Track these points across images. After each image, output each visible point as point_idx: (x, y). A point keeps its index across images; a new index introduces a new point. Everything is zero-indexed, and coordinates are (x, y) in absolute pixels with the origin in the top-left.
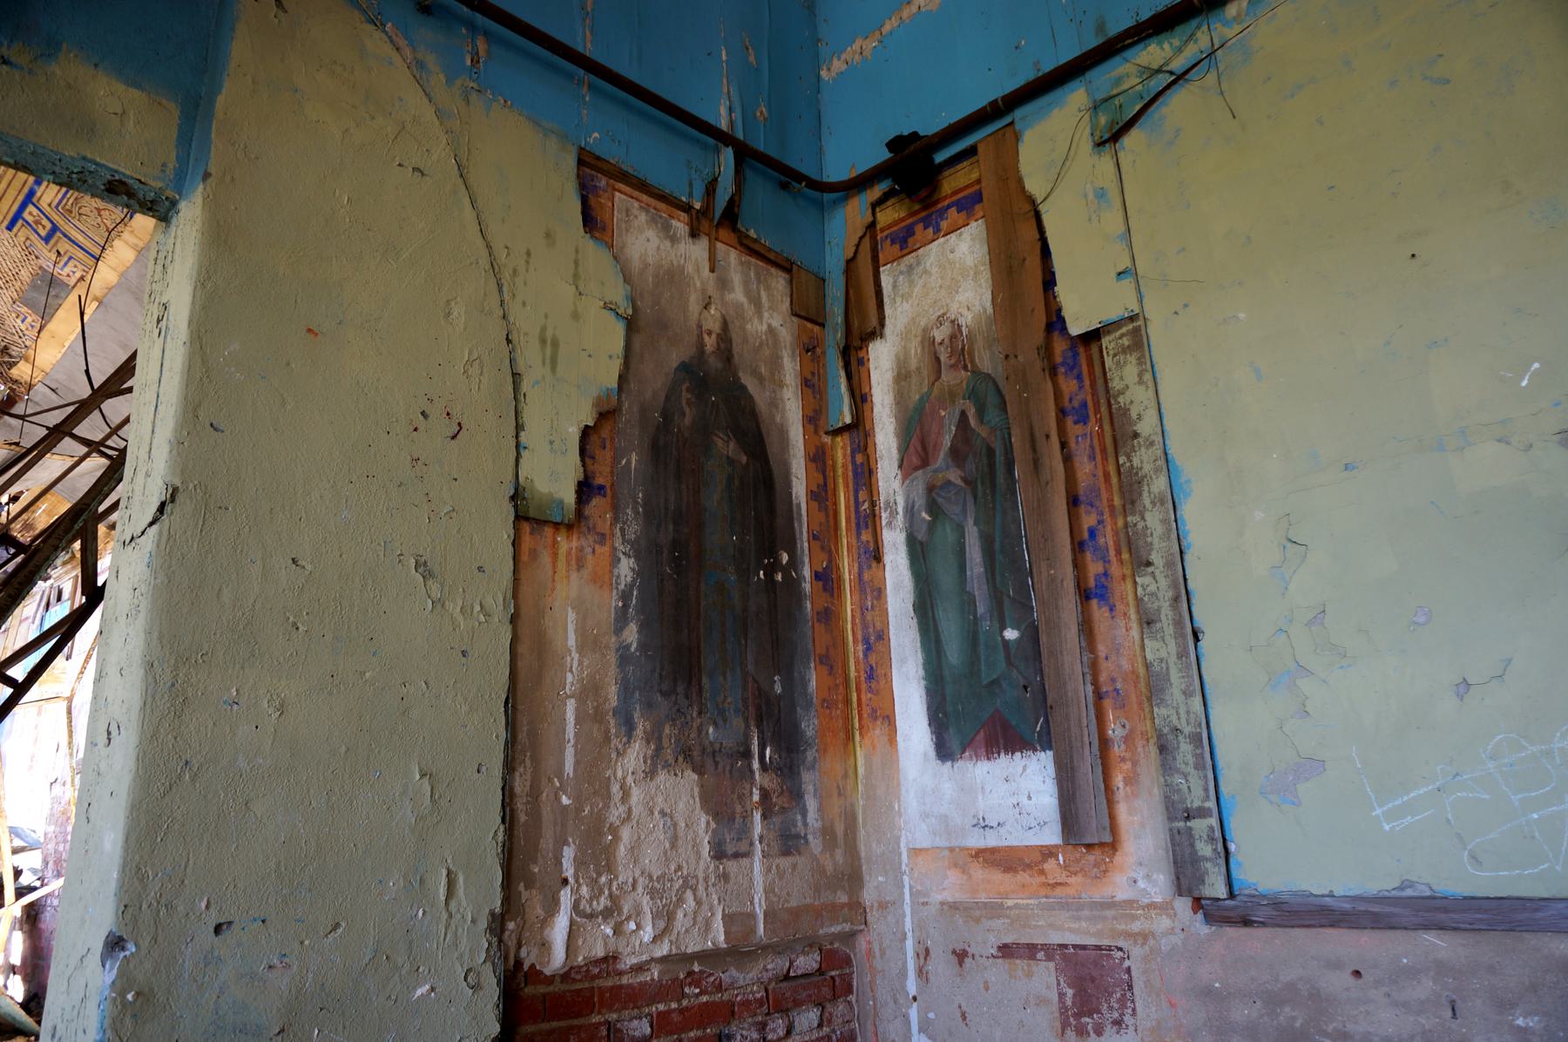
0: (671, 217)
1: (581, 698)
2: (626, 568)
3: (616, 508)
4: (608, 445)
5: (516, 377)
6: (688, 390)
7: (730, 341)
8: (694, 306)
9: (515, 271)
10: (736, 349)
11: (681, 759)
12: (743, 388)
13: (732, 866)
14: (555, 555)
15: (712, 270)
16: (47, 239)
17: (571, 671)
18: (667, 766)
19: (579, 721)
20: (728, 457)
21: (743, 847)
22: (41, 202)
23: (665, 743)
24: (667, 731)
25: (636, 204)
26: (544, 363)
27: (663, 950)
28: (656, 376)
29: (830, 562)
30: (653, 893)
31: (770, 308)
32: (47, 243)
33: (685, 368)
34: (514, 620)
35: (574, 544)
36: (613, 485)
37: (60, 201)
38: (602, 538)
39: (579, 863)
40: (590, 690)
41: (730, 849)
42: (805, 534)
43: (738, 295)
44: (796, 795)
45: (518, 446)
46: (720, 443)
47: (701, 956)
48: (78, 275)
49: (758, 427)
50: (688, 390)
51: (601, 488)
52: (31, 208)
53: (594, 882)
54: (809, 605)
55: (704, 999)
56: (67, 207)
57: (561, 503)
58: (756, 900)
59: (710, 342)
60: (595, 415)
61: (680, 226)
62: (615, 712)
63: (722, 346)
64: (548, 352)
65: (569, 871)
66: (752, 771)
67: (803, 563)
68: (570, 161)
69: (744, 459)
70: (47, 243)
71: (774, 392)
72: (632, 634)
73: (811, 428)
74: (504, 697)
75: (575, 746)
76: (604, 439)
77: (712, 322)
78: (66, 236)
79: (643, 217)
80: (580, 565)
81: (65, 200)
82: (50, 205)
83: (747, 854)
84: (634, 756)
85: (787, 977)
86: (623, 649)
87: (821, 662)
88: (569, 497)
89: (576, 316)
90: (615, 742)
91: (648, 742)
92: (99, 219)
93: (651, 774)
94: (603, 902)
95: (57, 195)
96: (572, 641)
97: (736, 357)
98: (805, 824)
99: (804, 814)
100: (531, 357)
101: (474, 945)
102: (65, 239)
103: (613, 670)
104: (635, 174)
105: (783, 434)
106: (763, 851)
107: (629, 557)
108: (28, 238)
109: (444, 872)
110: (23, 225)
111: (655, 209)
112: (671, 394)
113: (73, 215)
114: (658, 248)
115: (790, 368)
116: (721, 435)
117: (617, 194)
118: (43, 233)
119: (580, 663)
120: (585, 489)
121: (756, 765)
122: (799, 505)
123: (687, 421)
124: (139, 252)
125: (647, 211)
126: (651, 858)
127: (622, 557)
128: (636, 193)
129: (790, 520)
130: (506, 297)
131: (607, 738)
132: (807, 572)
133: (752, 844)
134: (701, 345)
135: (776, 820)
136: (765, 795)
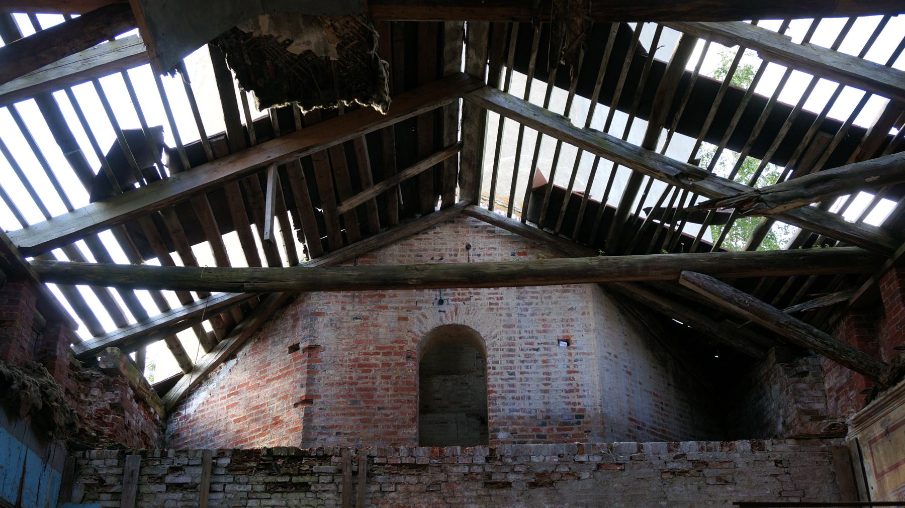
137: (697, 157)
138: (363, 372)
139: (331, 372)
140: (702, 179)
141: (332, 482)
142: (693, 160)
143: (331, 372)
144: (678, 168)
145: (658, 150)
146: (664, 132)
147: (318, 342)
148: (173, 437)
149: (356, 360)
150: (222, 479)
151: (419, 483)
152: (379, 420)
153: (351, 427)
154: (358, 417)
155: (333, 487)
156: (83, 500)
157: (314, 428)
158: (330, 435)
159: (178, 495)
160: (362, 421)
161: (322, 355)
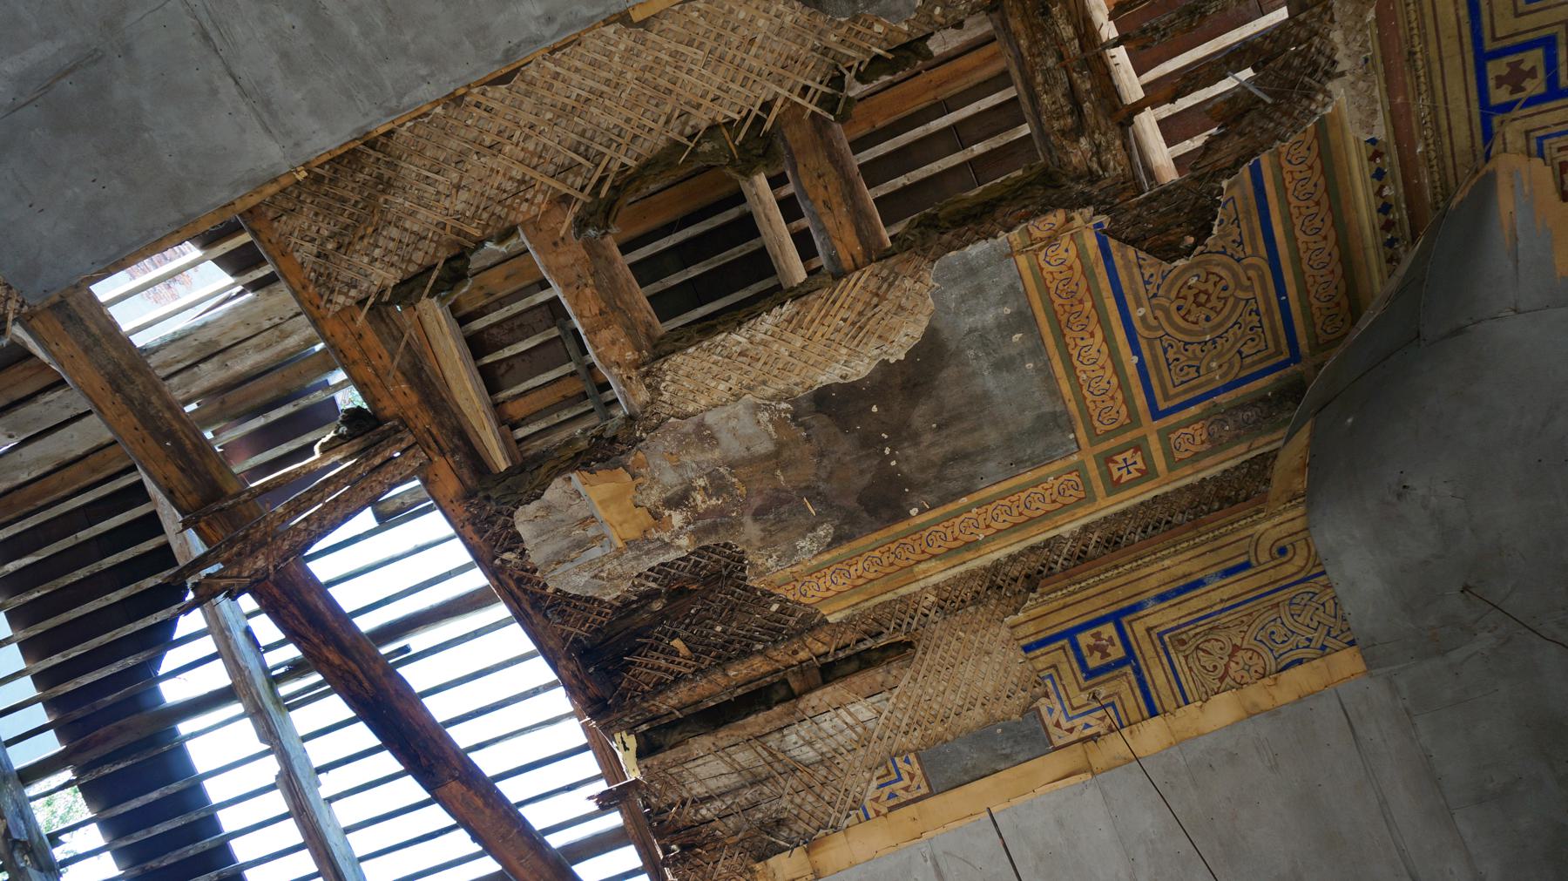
16: (1091, 674)
22: (1136, 625)
32: (1086, 679)
37: (1179, 627)
48: (1088, 732)
52: (1109, 630)
56: (1184, 636)
70: (1086, 679)
78: (1138, 671)
81: (1192, 626)
82: (1149, 630)
92: (1227, 659)
95: (1180, 618)
102: (1132, 678)
108: (1054, 666)
110: (1063, 648)
113: (1182, 648)
118: (1094, 661)
124: (1250, 715)
137: (63, 838)
140: (41, 870)
142: (54, 839)
144: (29, 832)
145: (31, 791)
146: (67, 775)
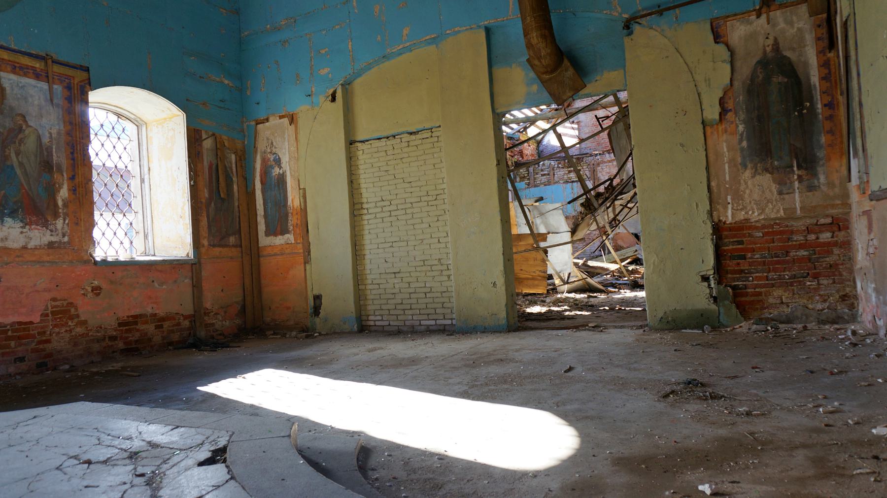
0: (749, 16)
1: (729, 162)
2: (741, 128)
3: (736, 113)
4: (732, 97)
5: (699, 95)
6: (761, 69)
7: (778, 44)
8: (761, 40)
9: (695, 67)
10: (781, 45)
11: (764, 171)
12: (785, 57)
13: (786, 196)
14: (718, 132)
15: (768, 24)
17: (726, 157)
18: (759, 174)
19: (729, 167)
20: (778, 82)
21: (791, 191)
23: (758, 168)
24: (759, 165)
25: (735, 21)
26: (706, 86)
27: (762, 217)
28: (745, 70)
29: (833, 98)
30: (757, 204)
31: (798, 21)
33: (759, 62)
34: (706, 150)
35: (723, 127)
36: (734, 108)
38: (732, 123)
39: (732, 199)
40: (732, 161)
41: (785, 192)
42: (818, 93)
43: (782, 25)
44: (815, 175)
45: (702, 110)
46: (775, 79)
47: (781, 219)
49: (793, 67)
50: (761, 69)
51: (730, 110)
53: (738, 205)
54: (820, 116)
55: (782, 229)
57: (715, 119)
58: (797, 204)
59: (768, 49)
60: (723, 93)
61: (754, 17)
62: (740, 164)
63: (775, 47)
64: (708, 83)
65: (729, 200)
66: (793, 171)
67: (817, 103)
68: (708, 26)
69: (786, 80)
71: (801, 51)
72: (745, 144)
73: (822, 55)
74: (705, 167)
75: (729, 174)
76: (730, 97)
77: (770, 42)
79: (738, 24)
80: (726, 131)
83: (793, 192)
84: (748, 173)
85: (816, 224)
86: (742, 150)
87: (828, 132)
88: (717, 117)
89: (714, 69)
90: (741, 171)
91: (752, 169)
93: (753, 177)
94: (741, 207)
96: (725, 150)
97: (781, 48)
98: (819, 183)
99: (818, 179)
100: (703, 88)
101: (704, 216)
103: (739, 154)
104: (731, 14)
105: (806, 65)
106: (799, 191)
107: (742, 124)
109: (695, 204)
111: (743, 18)
112: (754, 72)
114: (745, 30)
115: (809, 38)
116: (775, 77)
117: (728, 22)
119: (728, 154)
120: (724, 112)
121: (795, 169)
122: (815, 85)
123: (760, 78)
125: (739, 21)
126: (756, 196)
127: (739, 125)
128: (735, 18)
129: (810, 92)
130: (694, 75)
131: (738, 170)
132: (819, 106)
133: (794, 190)
134: (765, 52)
135: (805, 183)
136: (799, 177)
138: (596, 127)
139: (586, 129)
141: (587, 168)
143: (586, 129)
147: (580, 120)
148: (541, 152)
149: (593, 124)
150: (556, 171)
151: (613, 165)
152: (603, 143)
153: (594, 147)
154: (596, 143)
155: (588, 169)
156: (520, 181)
157: (582, 148)
158: (588, 150)
159: (545, 177)
160: (597, 144)
161: (582, 124)
